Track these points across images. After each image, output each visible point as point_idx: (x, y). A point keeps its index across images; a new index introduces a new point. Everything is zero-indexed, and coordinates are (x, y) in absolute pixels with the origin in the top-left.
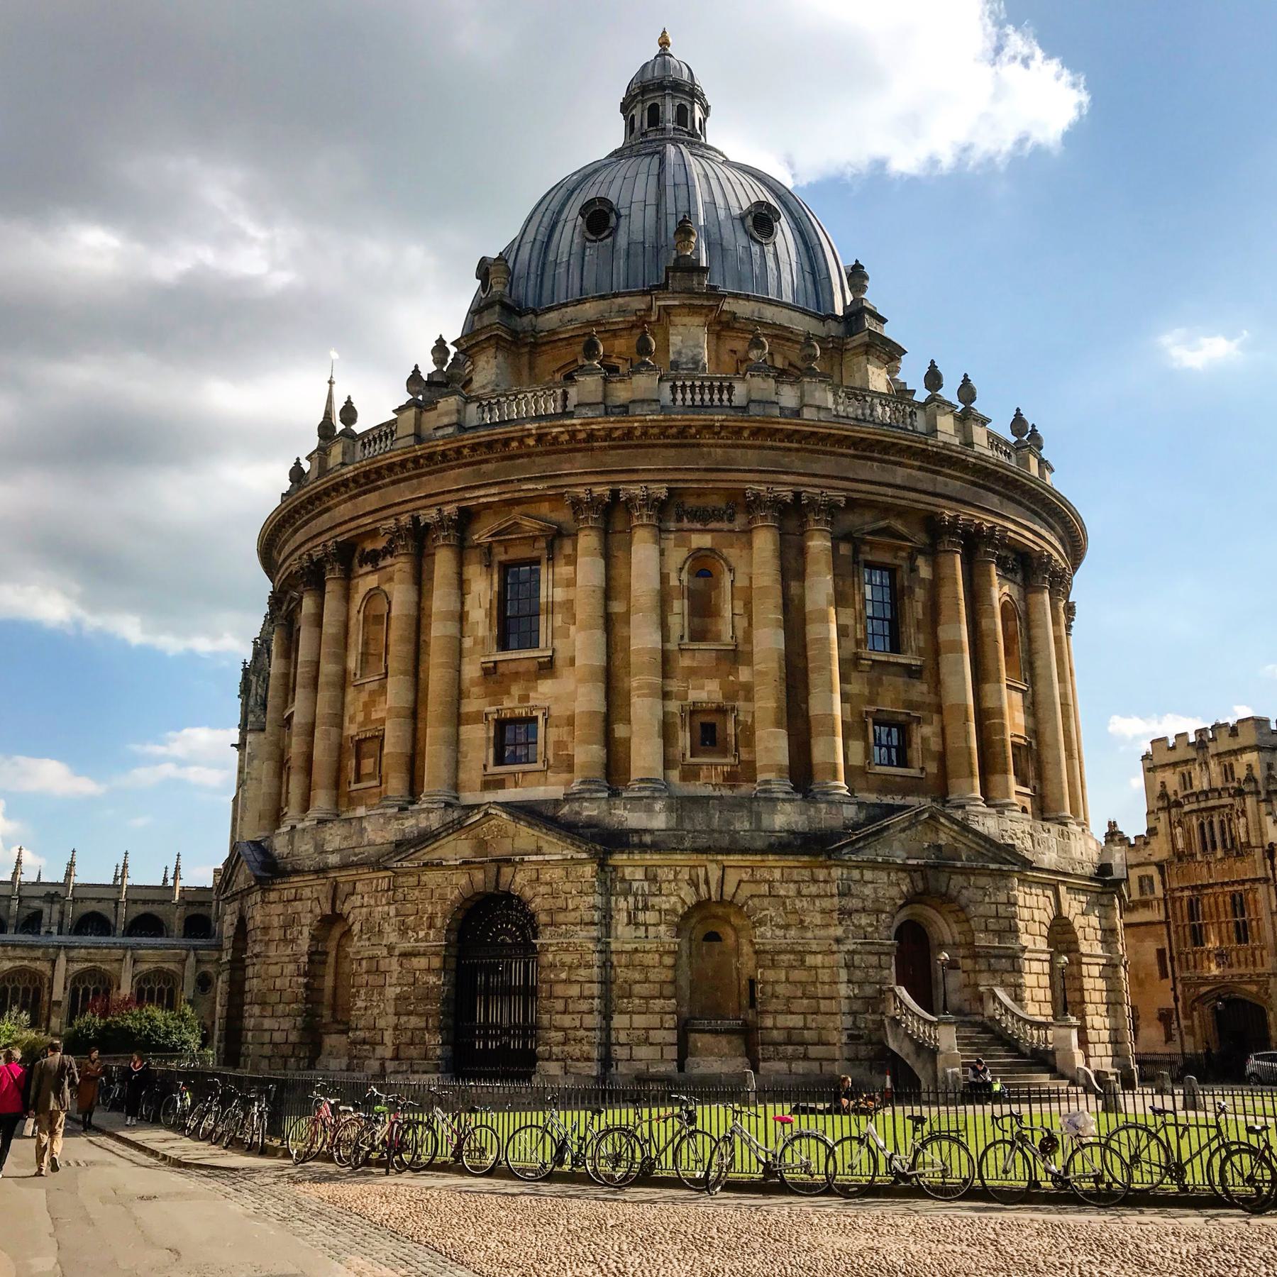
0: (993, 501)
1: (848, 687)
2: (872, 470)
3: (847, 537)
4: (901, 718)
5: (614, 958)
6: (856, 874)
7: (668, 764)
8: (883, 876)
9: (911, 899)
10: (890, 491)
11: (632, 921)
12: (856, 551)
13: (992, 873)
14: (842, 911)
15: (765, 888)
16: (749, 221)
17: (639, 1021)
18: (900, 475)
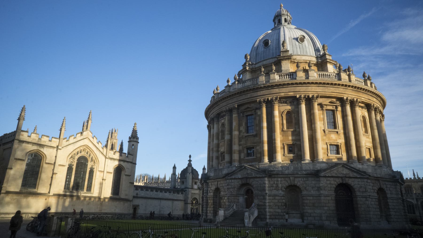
0: (277, 90)
1: (241, 143)
2: (244, 97)
3: (242, 112)
4: (251, 146)
5: (208, 199)
6: (230, 181)
7: (219, 163)
8: (236, 181)
9: (243, 185)
10: (246, 100)
11: (210, 192)
12: (243, 114)
13: (259, 177)
14: (228, 189)
15: (222, 185)
16: (263, 45)
17: (210, 209)
18: (249, 96)
